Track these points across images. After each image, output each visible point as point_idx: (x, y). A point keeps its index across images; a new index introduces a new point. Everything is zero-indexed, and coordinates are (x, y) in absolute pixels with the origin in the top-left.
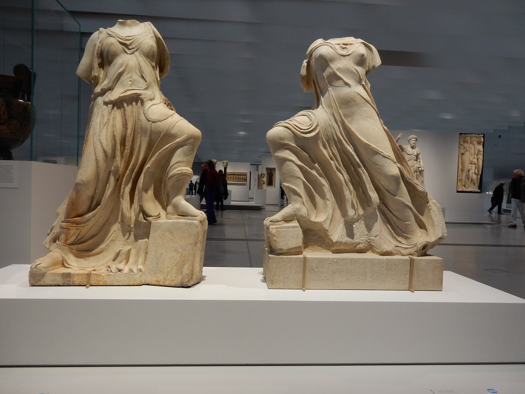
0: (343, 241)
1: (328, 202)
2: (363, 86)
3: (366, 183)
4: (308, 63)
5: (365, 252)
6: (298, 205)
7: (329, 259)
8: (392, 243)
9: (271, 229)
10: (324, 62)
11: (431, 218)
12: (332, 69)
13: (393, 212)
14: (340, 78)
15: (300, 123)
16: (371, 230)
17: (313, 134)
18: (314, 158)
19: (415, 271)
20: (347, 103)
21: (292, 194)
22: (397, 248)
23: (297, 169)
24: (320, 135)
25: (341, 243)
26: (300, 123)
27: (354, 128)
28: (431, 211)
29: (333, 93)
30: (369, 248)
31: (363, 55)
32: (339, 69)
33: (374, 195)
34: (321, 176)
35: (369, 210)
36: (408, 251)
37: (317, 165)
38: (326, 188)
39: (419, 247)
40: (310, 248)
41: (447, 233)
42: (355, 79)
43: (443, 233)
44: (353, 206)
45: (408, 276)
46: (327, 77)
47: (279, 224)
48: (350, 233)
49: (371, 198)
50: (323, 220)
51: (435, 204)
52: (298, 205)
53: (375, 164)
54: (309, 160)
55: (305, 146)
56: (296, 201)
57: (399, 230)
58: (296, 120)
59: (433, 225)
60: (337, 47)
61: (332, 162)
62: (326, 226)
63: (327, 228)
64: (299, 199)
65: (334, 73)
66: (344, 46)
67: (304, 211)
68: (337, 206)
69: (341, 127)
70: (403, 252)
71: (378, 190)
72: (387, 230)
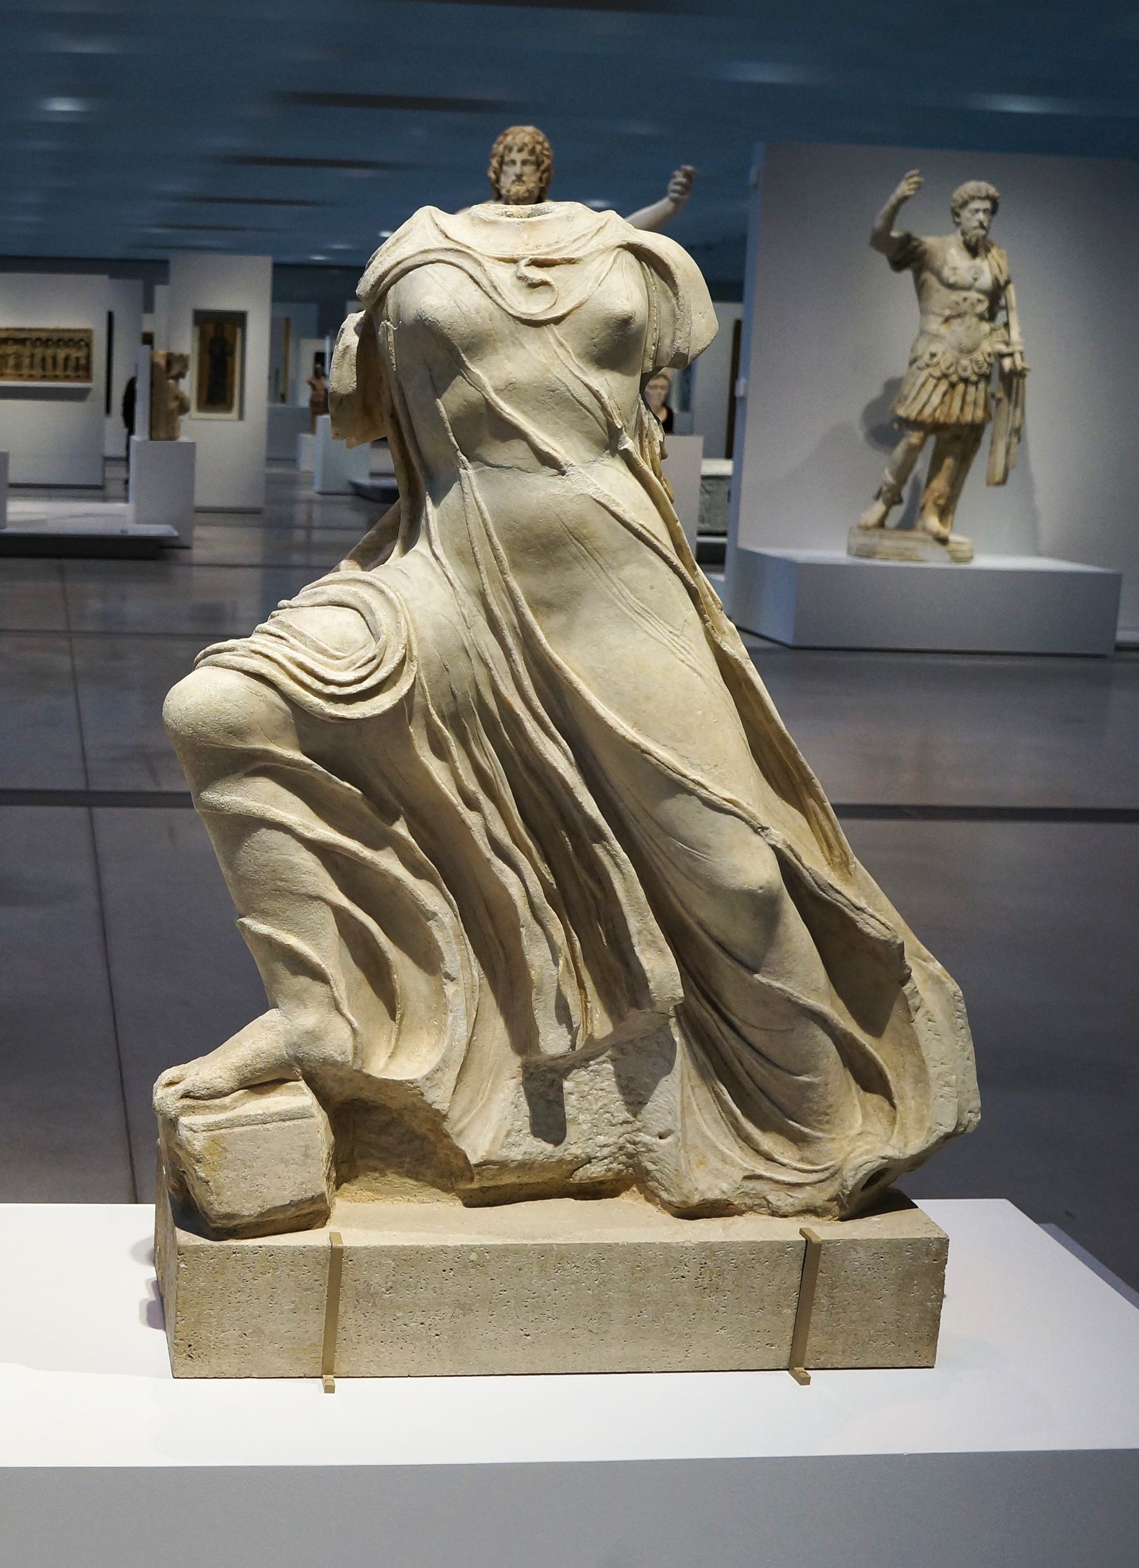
0: (516, 1154)
1: (450, 989)
2: (628, 459)
3: (627, 909)
4: (367, 331)
5: (613, 1193)
6: (309, 1018)
7: (443, 1250)
8: (733, 1164)
9: (184, 1133)
10: (442, 351)
11: (913, 1045)
12: (476, 384)
13: (745, 1030)
14: (512, 432)
15: (323, 652)
16: (642, 1104)
17: (384, 702)
18: (391, 797)
19: (821, 1295)
20: (548, 549)
21: (282, 971)
22: (750, 1184)
23: (308, 861)
24: (418, 699)
25: (503, 1166)
26: (323, 652)
27: (572, 661)
28: (918, 1017)
29: (477, 494)
30: (630, 1177)
31: (625, 322)
32: (510, 390)
33: (659, 966)
34: (418, 870)
35: (638, 1020)
36: (802, 1197)
37: (401, 828)
38: (442, 927)
39: (851, 1183)
40: (363, 1180)
41: (983, 1110)
42: (588, 435)
43: (960, 1111)
44: (563, 1013)
45: (789, 1312)
46: (456, 422)
47: (224, 1108)
48: (548, 1118)
49: (646, 981)
50: (426, 1070)
51: (938, 981)
52: (309, 1018)
53: (668, 831)
54: (365, 808)
55: (349, 758)
56: (300, 999)
57: (765, 1099)
58: (300, 636)
59: (921, 1077)
60: (504, 275)
61: (471, 818)
62: (439, 1098)
63: (442, 1106)
64: (318, 988)
65: (489, 407)
66: (537, 274)
67: (337, 1042)
68: (490, 1001)
69: (517, 656)
70: (777, 1198)
71: (679, 935)
72: (715, 1109)
